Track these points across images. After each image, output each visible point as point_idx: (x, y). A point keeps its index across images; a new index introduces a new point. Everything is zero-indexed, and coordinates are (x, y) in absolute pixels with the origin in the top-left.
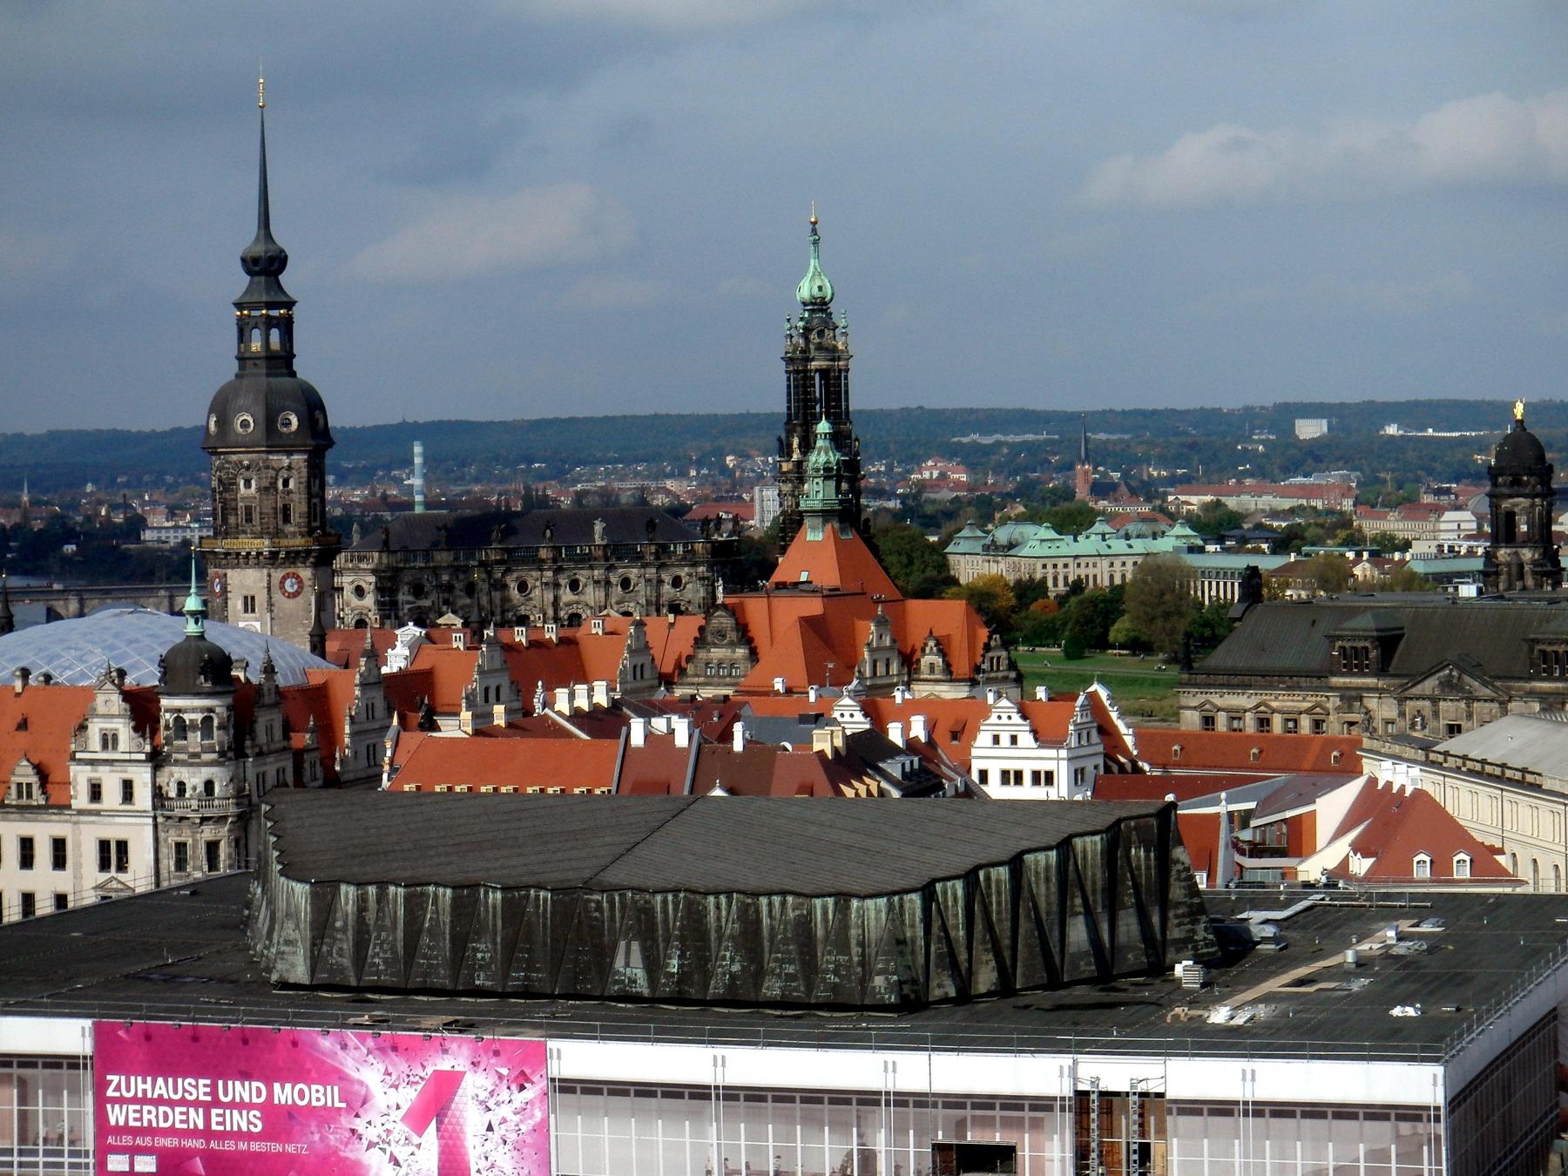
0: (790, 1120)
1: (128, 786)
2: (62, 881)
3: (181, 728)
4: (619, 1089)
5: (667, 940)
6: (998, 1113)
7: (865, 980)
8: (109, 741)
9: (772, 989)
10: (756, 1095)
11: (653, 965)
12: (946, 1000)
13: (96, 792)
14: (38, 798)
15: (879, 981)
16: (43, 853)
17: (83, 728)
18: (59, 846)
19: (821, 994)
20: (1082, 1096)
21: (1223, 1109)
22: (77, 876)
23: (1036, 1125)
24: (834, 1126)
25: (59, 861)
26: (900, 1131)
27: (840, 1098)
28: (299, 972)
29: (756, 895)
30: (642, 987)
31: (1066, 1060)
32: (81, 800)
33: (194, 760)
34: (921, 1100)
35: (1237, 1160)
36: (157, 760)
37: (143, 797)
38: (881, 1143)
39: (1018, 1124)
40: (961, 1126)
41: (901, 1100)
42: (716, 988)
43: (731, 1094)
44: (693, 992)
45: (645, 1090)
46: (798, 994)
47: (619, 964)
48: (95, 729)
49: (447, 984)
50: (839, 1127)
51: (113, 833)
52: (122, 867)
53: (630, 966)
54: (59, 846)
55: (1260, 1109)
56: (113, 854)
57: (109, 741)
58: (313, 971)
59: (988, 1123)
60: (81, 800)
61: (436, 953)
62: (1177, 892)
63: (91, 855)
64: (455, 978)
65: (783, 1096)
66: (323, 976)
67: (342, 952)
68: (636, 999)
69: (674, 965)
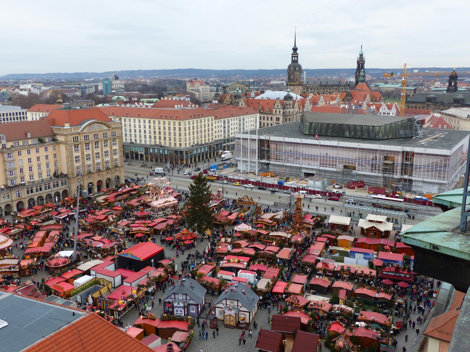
0: (367, 152)
1: (280, 111)
2: (271, 122)
3: (287, 105)
4: (346, 148)
5: (352, 131)
6: (393, 153)
7: (375, 137)
8: (278, 106)
9: (364, 137)
10: (363, 149)
11: (350, 133)
12: (385, 139)
13: (276, 111)
14: (269, 112)
15: (377, 136)
16: (270, 119)
17: (275, 104)
18: (271, 118)
19: (370, 138)
20: (403, 151)
21: (421, 154)
22: (273, 121)
23: (397, 155)
24: (369, 152)
25: (271, 120)
26: (380, 154)
27: (373, 150)
28: (307, 133)
29: (363, 126)
30: (348, 136)
31: (402, 147)
32: (274, 113)
33: (288, 108)
34: (383, 151)
35: (423, 160)
36: (284, 108)
37: (282, 113)
38: (378, 156)
39: (395, 154)
40: (388, 154)
41: (381, 150)
42: (357, 136)
43: (360, 149)
44: (354, 137)
45: (350, 148)
46: (367, 138)
47: (346, 133)
48: (276, 105)
49: (325, 135)
50: (373, 154)
51: (278, 117)
52: (279, 120)
53: (347, 134)
54: (271, 118)
55: (426, 154)
56: (278, 119)
57: (278, 106)
58: (309, 133)
59: (392, 154)
60: (274, 113)
61: (323, 132)
62: (414, 128)
63: (275, 119)
64: (326, 134)
65: (366, 149)
66: (310, 134)
67: (312, 131)
68: (347, 137)
69: (352, 134)
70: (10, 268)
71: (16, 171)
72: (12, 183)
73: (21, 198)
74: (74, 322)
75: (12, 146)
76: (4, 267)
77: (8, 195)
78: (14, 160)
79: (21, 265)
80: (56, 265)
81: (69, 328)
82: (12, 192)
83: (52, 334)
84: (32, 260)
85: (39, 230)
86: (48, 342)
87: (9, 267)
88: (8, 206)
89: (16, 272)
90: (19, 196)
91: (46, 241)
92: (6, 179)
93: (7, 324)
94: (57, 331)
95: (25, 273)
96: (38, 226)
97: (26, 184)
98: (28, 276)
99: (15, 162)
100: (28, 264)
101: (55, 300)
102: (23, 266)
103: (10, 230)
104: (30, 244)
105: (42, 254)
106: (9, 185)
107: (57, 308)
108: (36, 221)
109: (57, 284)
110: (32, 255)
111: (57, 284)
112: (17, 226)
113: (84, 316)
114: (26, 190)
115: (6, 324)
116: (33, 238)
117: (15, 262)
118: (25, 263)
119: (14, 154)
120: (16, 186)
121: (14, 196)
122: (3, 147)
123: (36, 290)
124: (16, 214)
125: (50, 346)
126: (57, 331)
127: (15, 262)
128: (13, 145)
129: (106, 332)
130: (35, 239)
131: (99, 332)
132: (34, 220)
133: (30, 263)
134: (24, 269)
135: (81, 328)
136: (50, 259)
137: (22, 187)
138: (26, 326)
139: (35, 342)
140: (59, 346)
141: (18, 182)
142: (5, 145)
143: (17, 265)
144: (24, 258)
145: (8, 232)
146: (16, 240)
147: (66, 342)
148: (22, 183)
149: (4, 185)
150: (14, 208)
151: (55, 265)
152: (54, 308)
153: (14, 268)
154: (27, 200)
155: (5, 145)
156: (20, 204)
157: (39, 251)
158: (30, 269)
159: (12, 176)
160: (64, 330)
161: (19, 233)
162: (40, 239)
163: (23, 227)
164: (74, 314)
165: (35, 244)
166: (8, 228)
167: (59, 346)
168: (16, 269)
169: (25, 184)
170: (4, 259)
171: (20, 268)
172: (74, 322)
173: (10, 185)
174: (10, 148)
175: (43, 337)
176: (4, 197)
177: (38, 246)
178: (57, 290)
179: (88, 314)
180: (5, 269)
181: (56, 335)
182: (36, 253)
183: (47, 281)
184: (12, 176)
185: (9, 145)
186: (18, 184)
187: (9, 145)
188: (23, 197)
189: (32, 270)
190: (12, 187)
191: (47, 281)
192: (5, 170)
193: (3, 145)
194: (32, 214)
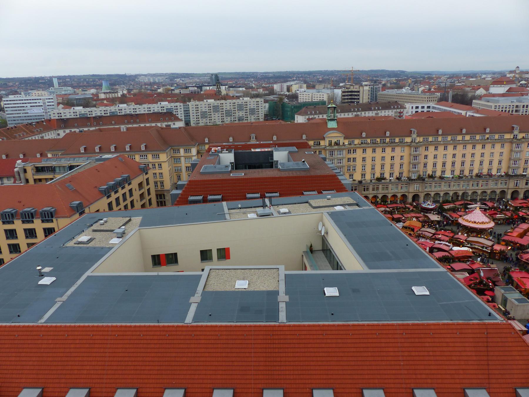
70: (483, 247)
71: (520, 161)
72: (513, 172)
73: (517, 188)
74: (486, 321)
75: (523, 137)
76: (478, 244)
77: (506, 183)
78: (521, 151)
79: (493, 248)
80: (527, 261)
81: (478, 324)
82: (510, 180)
83: (460, 322)
84: (506, 247)
85: (524, 222)
86: (453, 327)
87: (482, 245)
88: (503, 192)
89: (488, 252)
90: (516, 186)
91: (527, 235)
92: (509, 167)
93: (429, 294)
94: (466, 322)
95: (495, 257)
96: (525, 218)
97: (527, 176)
98: (497, 260)
99: (522, 153)
100: (500, 250)
101: (513, 292)
102: (495, 250)
103: (497, 214)
104: (510, 232)
105: (518, 245)
106: (510, 173)
107: (478, 301)
108: (525, 213)
109: (521, 278)
110: (507, 243)
111: (521, 278)
112: (504, 212)
113: (499, 322)
114: (525, 181)
115: (428, 293)
116: (515, 227)
117: (490, 243)
118: (497, 247)
119: (523, 145)
120: (516, 176)
121: (512, 184)
122: (514, 137)
123: (498, 275)
124: (508, 201)
125: (455, 331)
126: (466, 322)
127: (490, 243)
128: (525, 136)
129: (519, 349)
130: (516, 229)
131: (510, 344)
132: (524, 211)
133: (502, 249)
134: (496, 253)
135: (491, 331)
136: (524, 253)
137: (522, 178)
138: (442, 303)
139: (443, 320)
140: (463, 336)
141: (520, 172)
142: (516, 135)
143: (490, 246)
144: (499, 243)
145: (493, 216)
146: (499, 224)
147: (471, 336)
148: (523, 174)
149: (504, 173)
150: (508, 195)
151: (527, 260)
152: (475, 299)
153: (486, 248)
154: (523, 191)
155: (516, 135)
156: (515, 194)
157: (516, 241)
158: (500, 255)
159: (515, 166)
160: (473, 324)
161: (503, 219)
162: (521, 231)
163: (510, 215)
164: (490, 314)
165: (515, 234)
166: (495, 212)
167: (463, 336)
168: (488, 250)
169: (525, 175)
170: (480, 237)
171: (492, 250)
172: (486, 321)
173: (510, 173)
174: (521, 139)
175: (451, 320)
176: (501, 183)
177: (517, 236)
178: (519, 284)
179: (504, 322)
180: (478, 246)
181: (463, 324)
182: (512, 242)
183: (513, 272)
184: (515, 166)
185: (520, 136)
186: (518, 174)
187: (520, 136)
188: (520, 187)
189: (502, 257)
190: (512, 176)
191: (513, 272)
192: (510, 159)
193: (514, 135)
194: (524, 205)
